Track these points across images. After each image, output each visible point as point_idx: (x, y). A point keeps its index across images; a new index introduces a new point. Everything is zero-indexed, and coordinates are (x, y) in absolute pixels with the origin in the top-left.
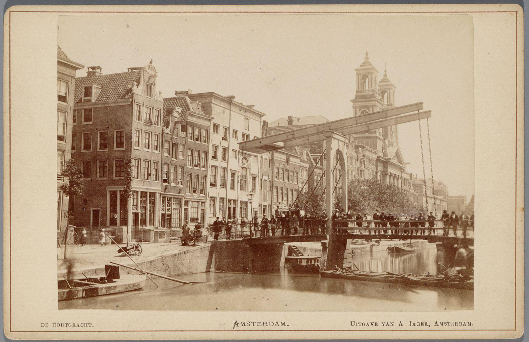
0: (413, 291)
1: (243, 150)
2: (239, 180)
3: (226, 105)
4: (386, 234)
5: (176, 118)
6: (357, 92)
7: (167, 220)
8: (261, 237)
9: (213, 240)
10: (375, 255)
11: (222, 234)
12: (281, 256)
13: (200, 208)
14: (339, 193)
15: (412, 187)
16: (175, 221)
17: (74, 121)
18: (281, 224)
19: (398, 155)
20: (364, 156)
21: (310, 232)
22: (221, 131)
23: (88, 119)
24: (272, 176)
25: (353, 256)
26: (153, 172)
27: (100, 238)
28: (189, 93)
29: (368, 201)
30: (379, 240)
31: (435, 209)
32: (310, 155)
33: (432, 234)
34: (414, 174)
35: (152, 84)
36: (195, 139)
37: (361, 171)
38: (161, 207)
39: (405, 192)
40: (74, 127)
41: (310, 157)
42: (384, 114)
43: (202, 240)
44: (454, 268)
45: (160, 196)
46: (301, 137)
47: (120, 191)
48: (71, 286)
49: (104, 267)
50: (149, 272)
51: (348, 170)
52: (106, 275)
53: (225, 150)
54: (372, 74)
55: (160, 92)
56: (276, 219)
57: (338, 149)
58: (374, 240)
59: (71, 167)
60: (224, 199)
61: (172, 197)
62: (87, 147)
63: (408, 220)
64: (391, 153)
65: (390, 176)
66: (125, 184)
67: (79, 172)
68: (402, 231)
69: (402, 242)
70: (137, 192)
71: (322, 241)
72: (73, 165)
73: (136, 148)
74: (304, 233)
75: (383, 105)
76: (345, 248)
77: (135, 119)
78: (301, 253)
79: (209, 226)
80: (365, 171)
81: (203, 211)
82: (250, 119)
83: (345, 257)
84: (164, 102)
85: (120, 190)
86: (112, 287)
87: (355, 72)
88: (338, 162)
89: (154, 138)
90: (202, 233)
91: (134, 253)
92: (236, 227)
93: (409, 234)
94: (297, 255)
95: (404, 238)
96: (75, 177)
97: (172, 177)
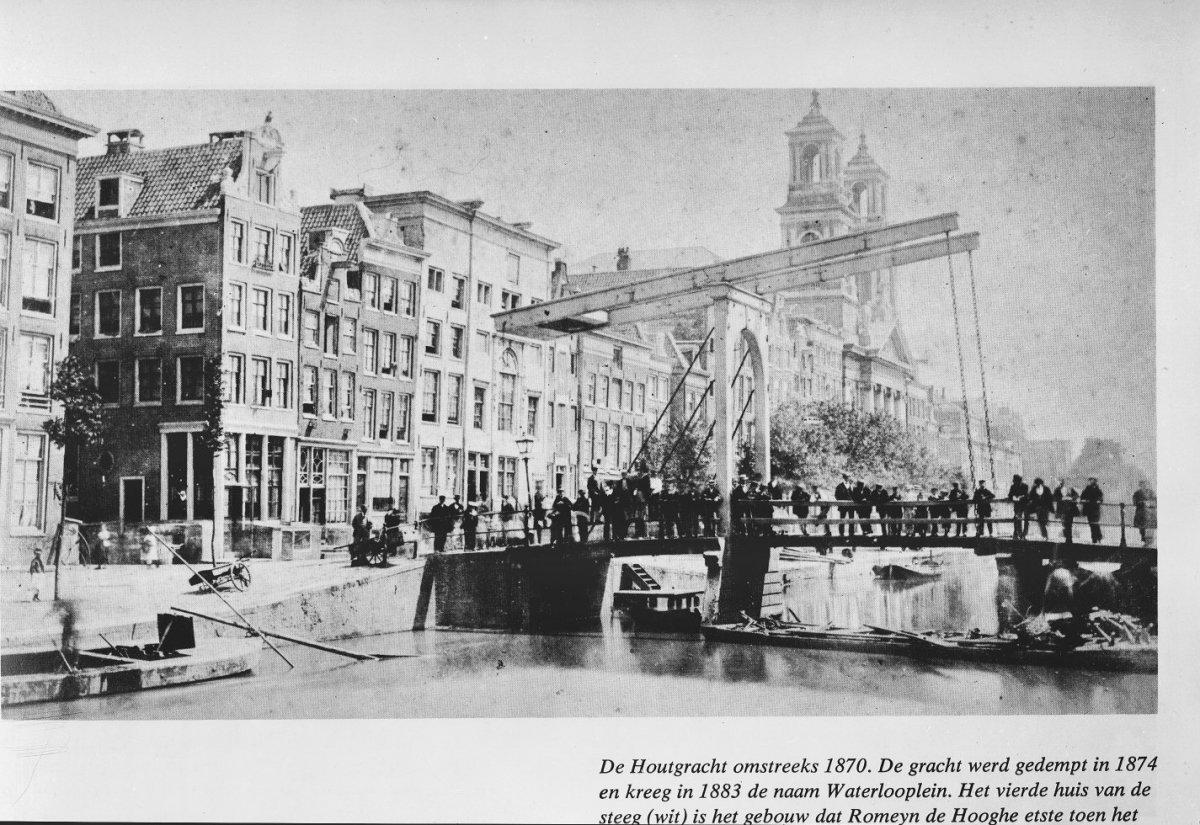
0: (938, 674)
1: (504, 331)
2: (496, 404)
3: (463, 224)
4: (870, 535)
5: (333, 256)
6: (792, 189)
7: (313, 504)
8: (552, 544)
9: (432, 551)
10: (841, 583)
11: (454, 538)
12: (602, 589)
13: (398, 473)
14: (749, 437)
15: (933, 420)
16: (334, 507)
17: (75, 264)
18: (603, 513)
19: (895, 339)
20: (810, 344)
21: (676, 530)
22: (450, 286)
23: (109, 257)
24: (580, 395)
25: (785, 588)
26: (276, 387)
27: (144, 551)
28: (367, 193)
29: (824, 455)
30: (851, 548)
31: (993, 475)
32: (674, 342)
33: (986, 533)
34: (937, 390)
35: (271, 172)
36: (382, 306)
37: (803, 380)
38: (299, 472)
39: (917, 431)
40: (75, 279)
41: (676, 347)
42: (861, 244)
43: (402, 552)
44: (1041, 616)
45: (296, 445)
46: (650, 300)
47: (194, 434)
48: (73, 666)
49: (156, 619)
50: (269, 631)
51: (771, 378)
52: (160, 638)
53: (459, 331)
54: (827, 142)
55: (292, 192)
56: (590, 501)
57: (746, 329)
58: (837, 551)
59: (69, 376)
60: (457, 451)
61: (326, 449)
62: (109, 326)
63: (925, 499)
64: (878, 340)
65: (878, 392)
66: (206, 418)
67: (87, 385)
68: (909, 525)
69: (909, 553)
70: (236, 436)
71: (707, 553)
72: (73, 370)
73: (235, 327)
74: (660, 534)
75: (856, 220)
76: (765, 569)
77: (231, 258)
78: (653, 582)
79: (421, 518)
80: (814, 382)
81: (404, 481)
82: (522, 257)
83: (766, 589)
84: (302, 215)
85: (194, 430)
86: (175, 667)
87: (786, 140)
88: (745, 358)
89: (278, 303)
90: (404, 535)
91: (230, 584)
92: (488, 519)
93: (928, 535)
94: (644, 587)
95: (914, 544)
96: (80, 401)
97: (325, 398)
